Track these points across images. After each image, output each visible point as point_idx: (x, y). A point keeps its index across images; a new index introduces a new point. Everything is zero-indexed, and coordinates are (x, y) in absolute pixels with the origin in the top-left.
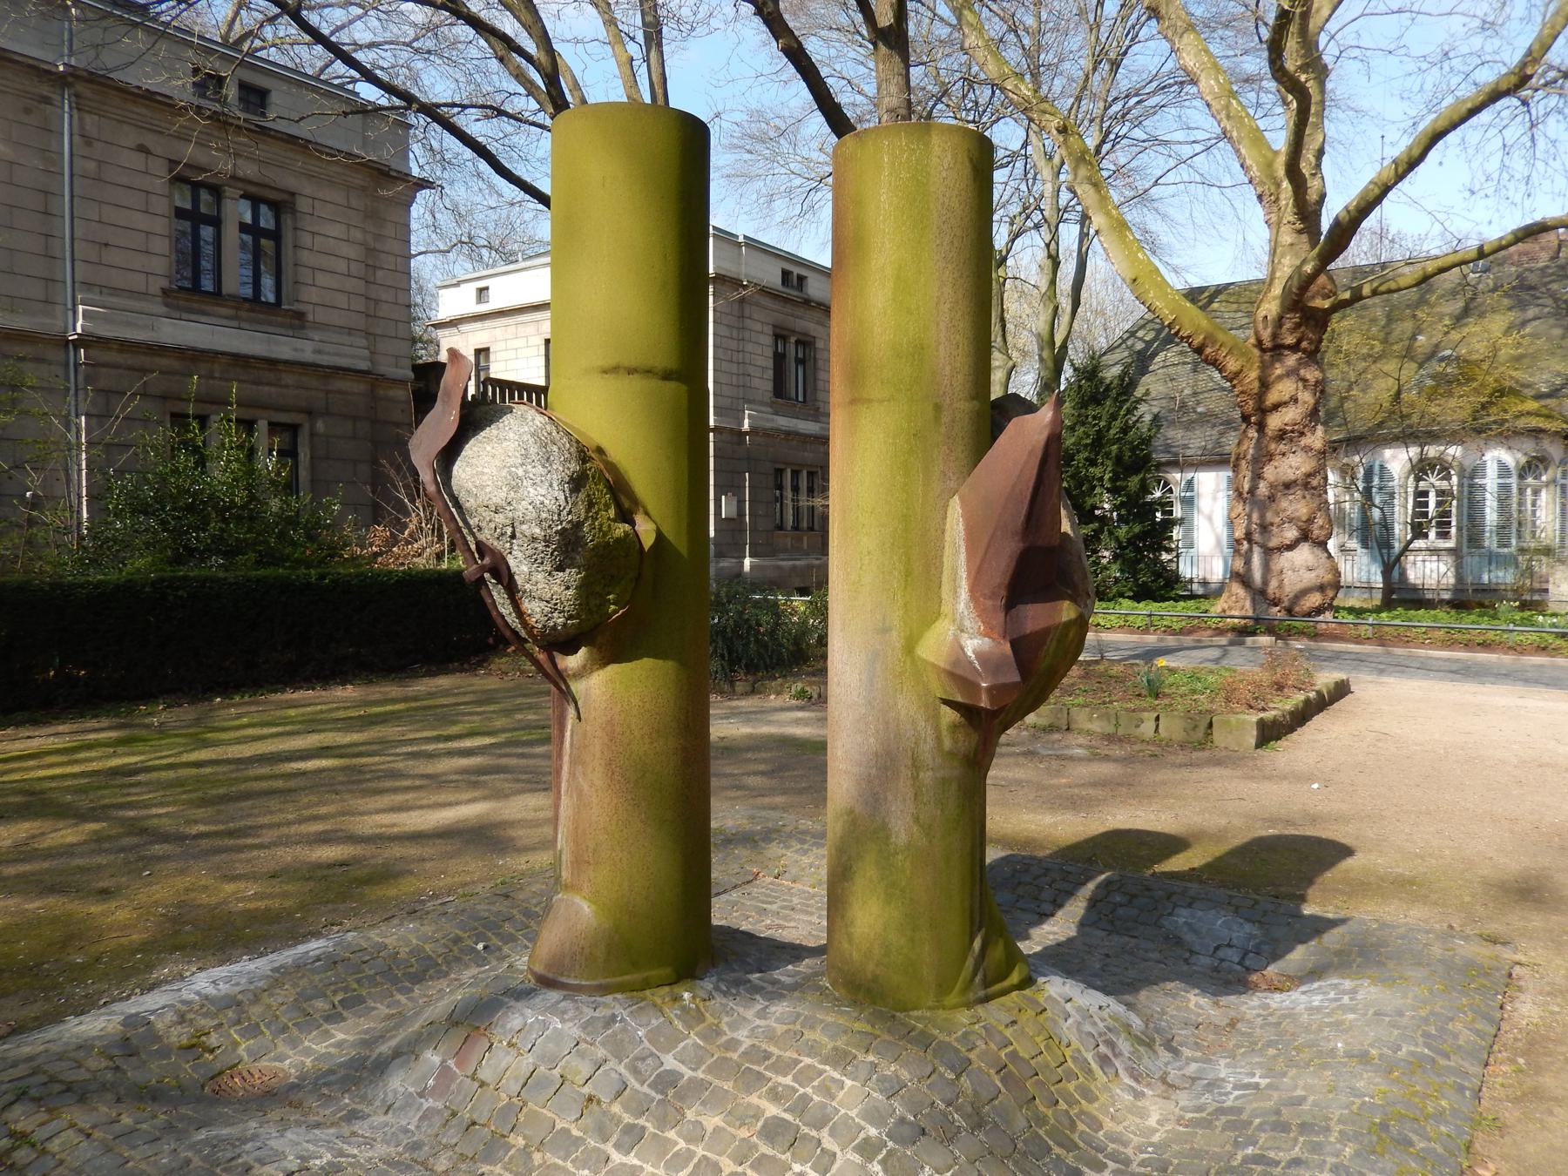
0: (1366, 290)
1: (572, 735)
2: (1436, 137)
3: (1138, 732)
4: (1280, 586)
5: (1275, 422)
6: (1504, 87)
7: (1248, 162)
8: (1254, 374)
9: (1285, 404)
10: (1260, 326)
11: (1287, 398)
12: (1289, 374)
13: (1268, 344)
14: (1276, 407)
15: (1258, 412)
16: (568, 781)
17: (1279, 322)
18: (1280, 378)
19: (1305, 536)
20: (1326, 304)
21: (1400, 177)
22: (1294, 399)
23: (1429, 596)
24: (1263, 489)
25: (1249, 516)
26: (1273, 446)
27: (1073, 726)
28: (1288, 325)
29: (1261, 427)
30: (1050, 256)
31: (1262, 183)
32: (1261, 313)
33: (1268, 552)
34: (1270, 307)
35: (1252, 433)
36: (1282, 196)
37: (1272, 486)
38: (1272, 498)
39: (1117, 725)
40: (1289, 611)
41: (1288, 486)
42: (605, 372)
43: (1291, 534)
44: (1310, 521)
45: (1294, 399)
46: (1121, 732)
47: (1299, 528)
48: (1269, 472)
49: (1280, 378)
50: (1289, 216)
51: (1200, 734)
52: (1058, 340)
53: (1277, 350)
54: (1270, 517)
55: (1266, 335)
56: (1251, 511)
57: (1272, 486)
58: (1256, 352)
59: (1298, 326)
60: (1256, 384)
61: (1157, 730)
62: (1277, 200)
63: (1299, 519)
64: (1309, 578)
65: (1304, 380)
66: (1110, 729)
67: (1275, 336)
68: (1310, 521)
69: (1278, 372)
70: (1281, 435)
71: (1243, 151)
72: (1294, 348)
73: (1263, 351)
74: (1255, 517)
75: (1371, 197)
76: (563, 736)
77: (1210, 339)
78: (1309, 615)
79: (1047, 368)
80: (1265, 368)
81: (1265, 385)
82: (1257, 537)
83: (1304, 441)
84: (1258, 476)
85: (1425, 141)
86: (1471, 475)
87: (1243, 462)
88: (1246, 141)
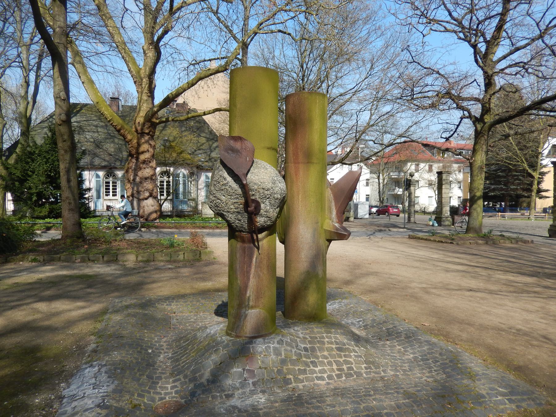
0: (170, 119)
1: (256, 259)
2: (201, 79)
3: (178, 259)
4: (144, 212)
5: (142, 157)
6: (220, 70)
7: (132, 70)
8: (135, 141)
9: (145, 152)
10: (137, 125)
11: (146, 150)
12: (147, 142)
13: (139, 131)
14: (143, 152)
15: (135, 154)
16: (254, 274)
17: (144, 124)
18: (144, 143)
19: (151, 195)
20: (157, 121)
21: (189, 88)
22: (148, 151)
23: (186, 213)
24: (138, 179)
25: (133, 188)
26: (141, 165)
27: (155, 259)
28: (146, 126)
29: (137, 159)
30: (26, 82)
31: (136, 78)
32: (137, 121)
33: (139, 200)
34: (140, 119)
35: (134, 160)
36: (143, 84)
37: (141, 178)
38: (141, 182)
39: (171, 257)
40: (146, 220)
41: (146, 179)
42: (268, 148)
43: (147, 194)
44: (153, 190)
45: (148, 151)
46: (172, 259)
47: (150, 193)
48: (140, 174)
49: (144, 143)
50: (146, 90)
51: (198, 257)
52: (28, 115)
53: (142, 134)
54: (140, 189)
55: (139, 128)
56: (134, 187)
57: (141, 178)
58: (136, 133)
59: (150, 127)
60: (136, 144)
61: (184, 257)
62: (141, 85)
63: (149, 190)
64: (152, 209)
65: (151, 145)
66: (168, 259)
67: (142, 129)
68: (153, 190)
69: (143, 141)
70: (144, 162)
71: (130, 65)
72: (148, 134)
73: (138, 133)
74: (135, 188)
75: (180, 92)
76: (252, 260)
77: (122, 127)
78: (153, 221)
79: (24, 126)
80: (139, 139)
81: (139, 145)
82: (135, 195)
83: (151, 164)
84: (136, 175)
85: (197, 79)
86: (177, 176)
87: (130, 170)
88: (131, 62)
